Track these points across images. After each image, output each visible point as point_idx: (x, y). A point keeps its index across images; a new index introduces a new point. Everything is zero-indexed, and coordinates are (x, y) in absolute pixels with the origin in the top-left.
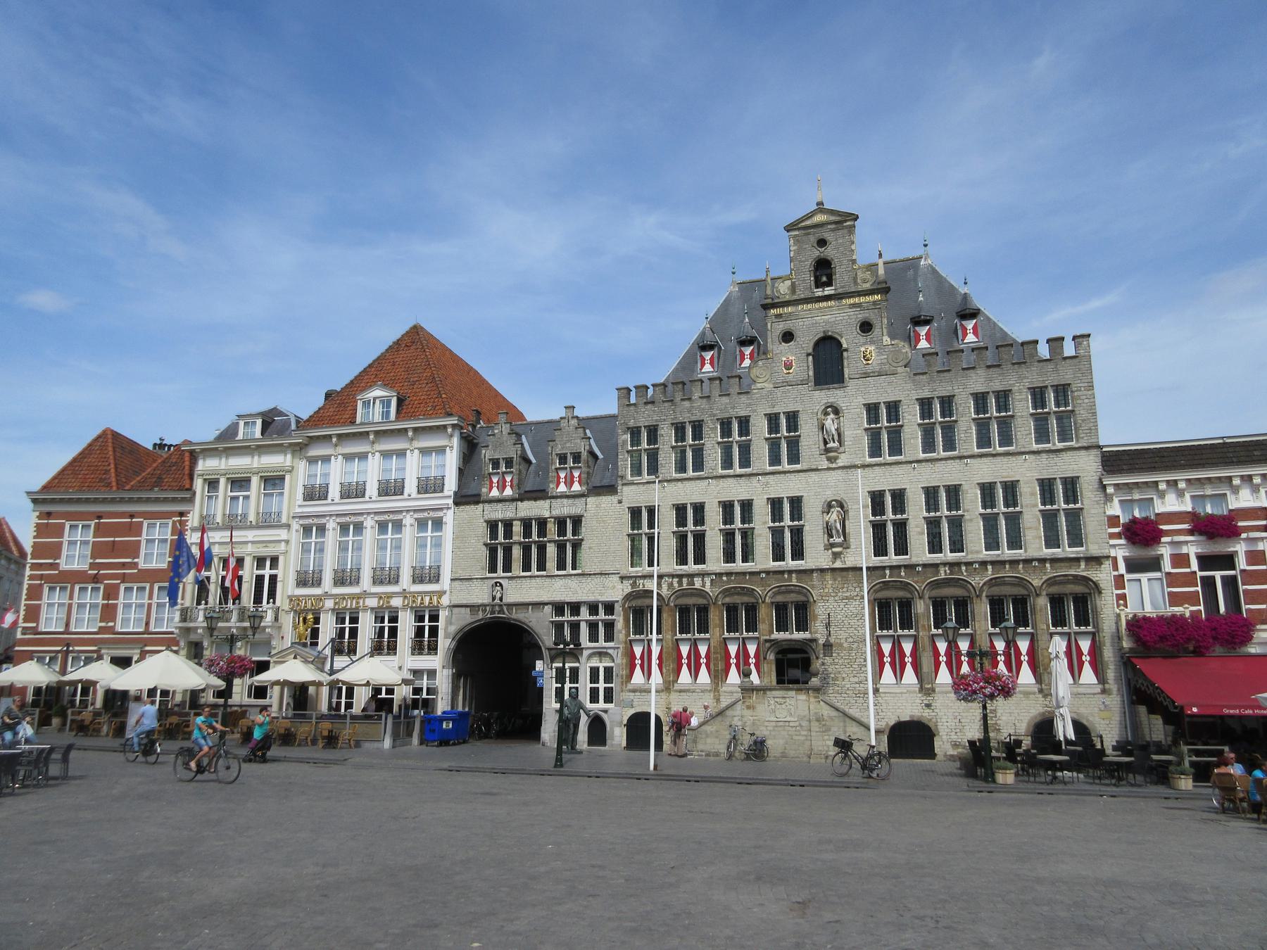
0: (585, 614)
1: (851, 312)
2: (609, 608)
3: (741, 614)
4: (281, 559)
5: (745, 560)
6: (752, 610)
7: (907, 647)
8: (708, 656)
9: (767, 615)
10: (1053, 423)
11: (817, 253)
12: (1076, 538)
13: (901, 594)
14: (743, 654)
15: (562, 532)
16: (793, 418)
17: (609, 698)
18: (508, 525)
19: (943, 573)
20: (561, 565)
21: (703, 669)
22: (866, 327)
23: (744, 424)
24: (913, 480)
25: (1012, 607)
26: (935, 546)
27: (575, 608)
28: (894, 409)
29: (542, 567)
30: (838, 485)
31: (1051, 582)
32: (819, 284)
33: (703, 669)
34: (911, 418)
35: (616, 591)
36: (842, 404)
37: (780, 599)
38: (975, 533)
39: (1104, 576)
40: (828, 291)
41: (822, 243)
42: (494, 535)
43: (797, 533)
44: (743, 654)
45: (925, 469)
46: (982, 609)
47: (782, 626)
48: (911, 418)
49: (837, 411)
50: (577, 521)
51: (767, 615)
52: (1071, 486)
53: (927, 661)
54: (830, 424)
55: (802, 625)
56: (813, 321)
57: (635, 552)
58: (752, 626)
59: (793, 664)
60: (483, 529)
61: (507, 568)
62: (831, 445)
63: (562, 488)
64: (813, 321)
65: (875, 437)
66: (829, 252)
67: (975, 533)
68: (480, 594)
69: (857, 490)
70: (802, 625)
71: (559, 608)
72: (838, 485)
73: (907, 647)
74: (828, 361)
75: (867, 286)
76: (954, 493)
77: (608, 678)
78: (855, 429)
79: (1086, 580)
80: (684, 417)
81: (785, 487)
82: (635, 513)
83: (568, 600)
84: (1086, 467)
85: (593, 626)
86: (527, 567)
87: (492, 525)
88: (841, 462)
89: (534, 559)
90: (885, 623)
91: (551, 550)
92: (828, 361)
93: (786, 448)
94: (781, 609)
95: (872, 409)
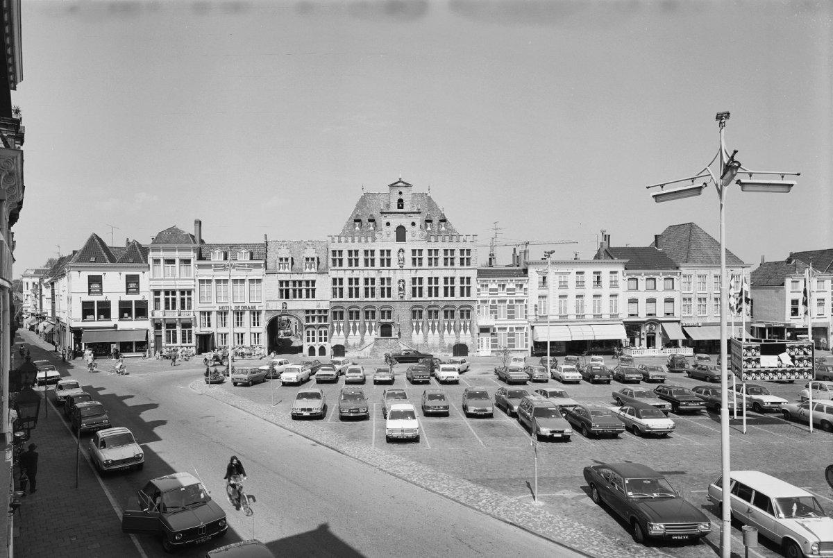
0: (316, 314)
1: (410, 219)
2: (326, 311)
3: (370, 314)
4: (193, 292)
5: (372, 297)
6: (373, 312)
7: (420, 324)
8: (359, 326)
9: (378, 314)
10: (465, 260)
11: (399, 197)
12: (468, 295)
13: (420, 309)
14: (370, 327)
15: (308, 285)
16: (389, 252)
17: (326, 340)
18: (287, 282)
19: (432, 303)
20: (308, 297)
21: (358, 331)
22: (413, 224)
23: (373, 252)
24: (425, 275)
25: (450, 313)
26: (430, 295)
27: (313, 311)
28: (420, 251)
29: (300, 297)
30: (401, 275)
31: (461, 307)
32: (399, 208)
33: (358, 331)
34: (425, 255)
35: (324, 306)
36: (404, 248)
37: (383, 309)
38: (441, 292)
39: (475, 306)
40: (400, 210)
41: (400, 193)
42: (281, 285)
43: (389, 289)
44: (370, 327)
45: (429, 272)
46: (441, 314)
47: (383, 318)
48: (425, 255)
49: (403, 251)
50: (313, 282)
51: (378, 314)
52: (469, 279)
53: (426, 328)
54: (401, 256)
55: (389, 317)
56: (396, 221)
57: (335, 293)
58: (373, 317)
59: (386, 330)
60: (278, 283)
61: (287, 297)
62: (401, 262)
63: (308, 270)
64: (396, 221)
65: (414, 260)
66: (402, 197)
67: (441, 292)
68: (278, 306)
69: (408, 277)
70: (389, 317)
71: (307, 311)
72: (401, 275)
73: (420, 324)
74: (401, 234)
75: (415, 211)
76: (437, 279)
77: (326, 334)
78: (408, 256)
79: (470, 306)
80: (353, 248)
81: (385, 274)
82: (335, 280)
83: (311, 309)
84: (473, 274)
85: (320, 317)
86: (295, 297)
87: (281, 283)
88: (404, 268)
89: (298, 294)
90: (414, 317)
91: (304, 292)
92: (401, 234)
93: (386, 262)
94: (383, 312)
95: (414, 251)
